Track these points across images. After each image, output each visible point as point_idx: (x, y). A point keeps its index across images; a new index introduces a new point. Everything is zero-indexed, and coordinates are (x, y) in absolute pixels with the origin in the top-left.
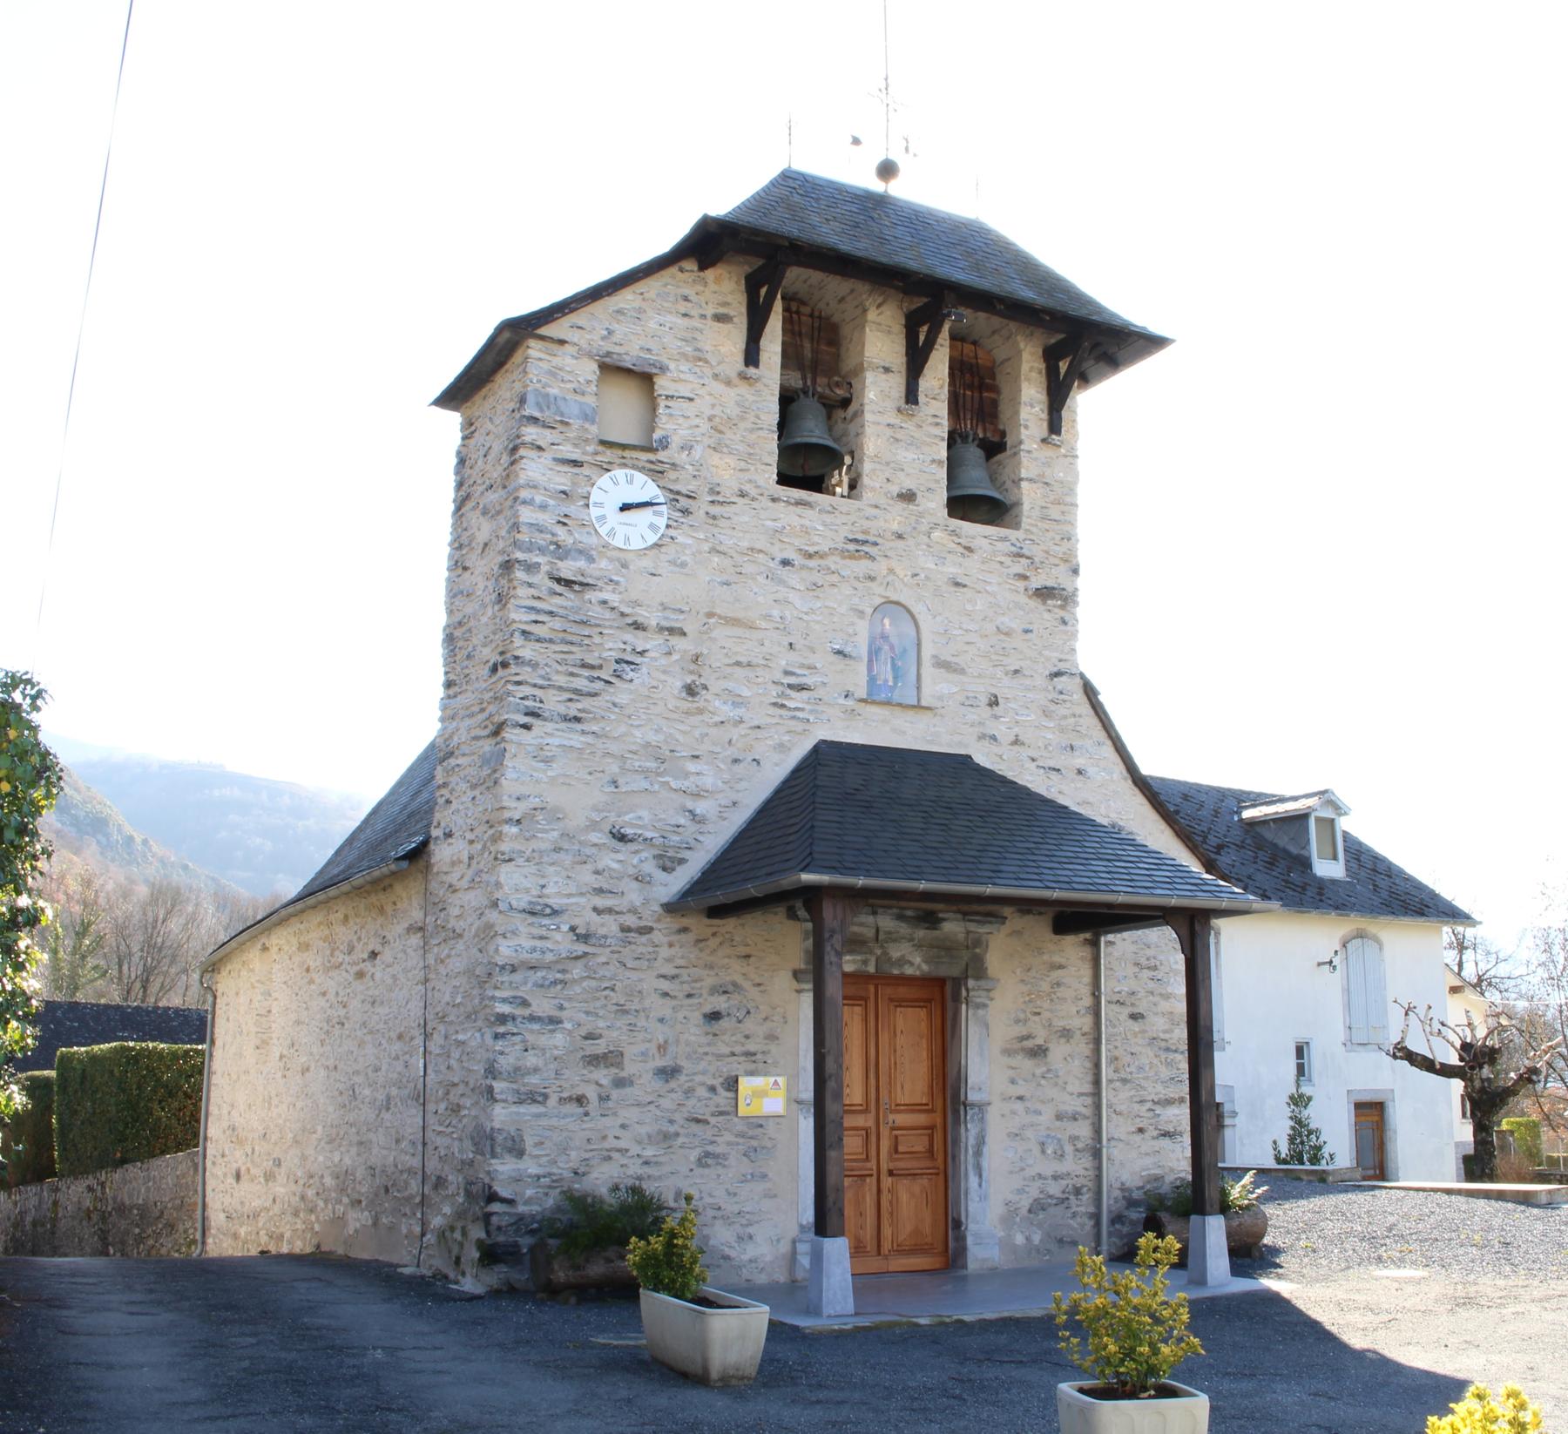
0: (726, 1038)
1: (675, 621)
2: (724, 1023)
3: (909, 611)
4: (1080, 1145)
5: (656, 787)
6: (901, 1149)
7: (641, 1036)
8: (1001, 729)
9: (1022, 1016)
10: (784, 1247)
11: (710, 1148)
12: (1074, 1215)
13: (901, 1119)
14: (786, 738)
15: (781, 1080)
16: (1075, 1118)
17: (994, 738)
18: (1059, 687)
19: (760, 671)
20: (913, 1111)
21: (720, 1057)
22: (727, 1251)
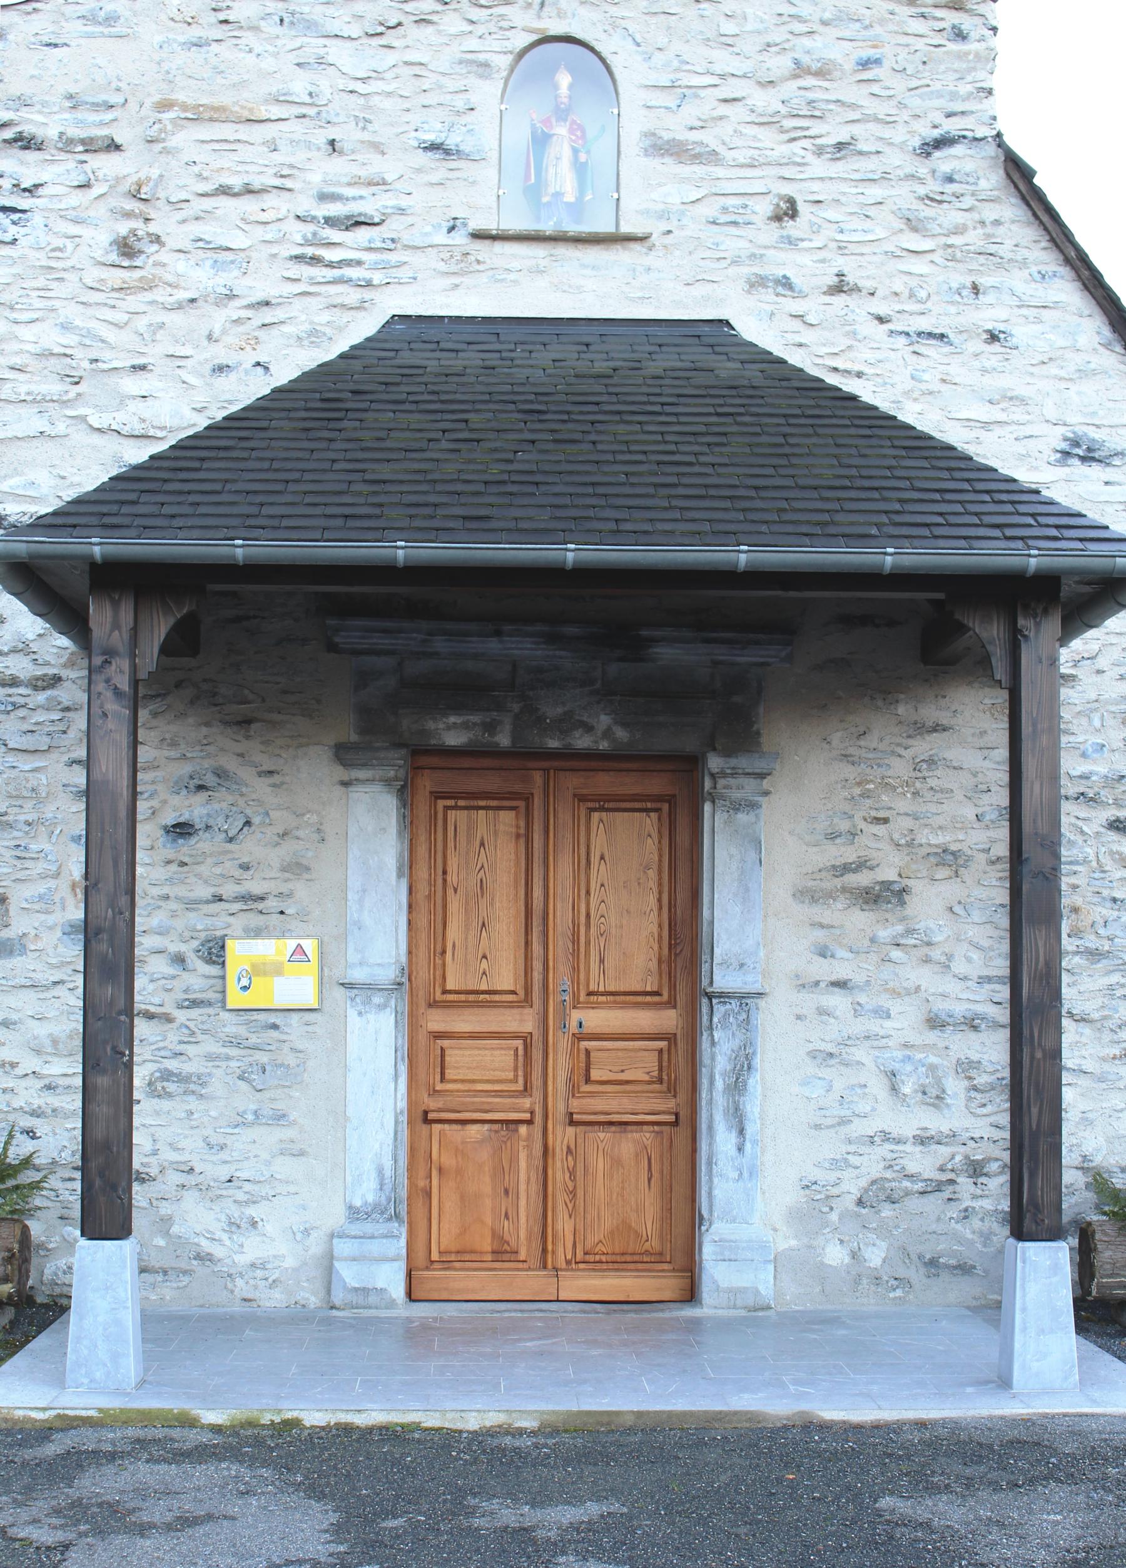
0: (203, 869)
1: (92, 125)
2: (202, 843)
3: (592, 49)
4: (982, 1080)
5: (61, 428)
6: (595, 1075)
7: (40, 867)
8: (806, 268)
9: (844, 826)
10: (315, 1246)
11: (172, 1065)
12: (966, 1214)
13: (596, 1019)
14: (325, 317)
15: (310, 946)
16: (972, 1024)
17: (786, 283)
18: (945, 168)
19: (270, 200)
20: (624, 1006)
21: (191, 905)
22: (206, 1245)
